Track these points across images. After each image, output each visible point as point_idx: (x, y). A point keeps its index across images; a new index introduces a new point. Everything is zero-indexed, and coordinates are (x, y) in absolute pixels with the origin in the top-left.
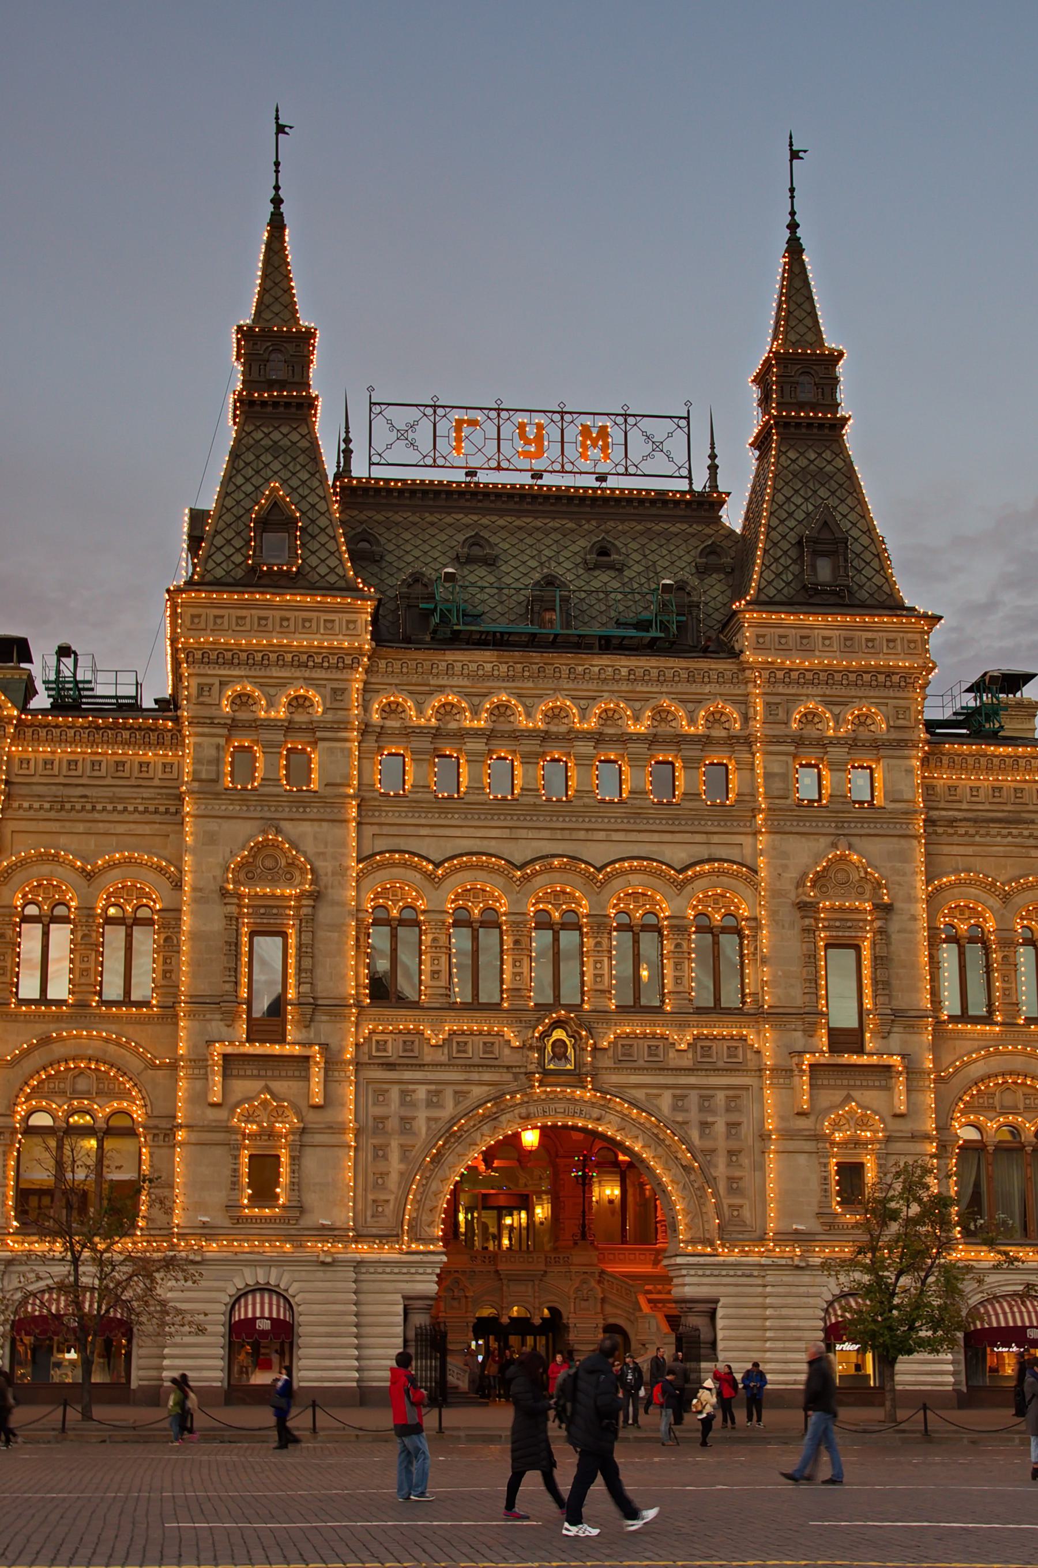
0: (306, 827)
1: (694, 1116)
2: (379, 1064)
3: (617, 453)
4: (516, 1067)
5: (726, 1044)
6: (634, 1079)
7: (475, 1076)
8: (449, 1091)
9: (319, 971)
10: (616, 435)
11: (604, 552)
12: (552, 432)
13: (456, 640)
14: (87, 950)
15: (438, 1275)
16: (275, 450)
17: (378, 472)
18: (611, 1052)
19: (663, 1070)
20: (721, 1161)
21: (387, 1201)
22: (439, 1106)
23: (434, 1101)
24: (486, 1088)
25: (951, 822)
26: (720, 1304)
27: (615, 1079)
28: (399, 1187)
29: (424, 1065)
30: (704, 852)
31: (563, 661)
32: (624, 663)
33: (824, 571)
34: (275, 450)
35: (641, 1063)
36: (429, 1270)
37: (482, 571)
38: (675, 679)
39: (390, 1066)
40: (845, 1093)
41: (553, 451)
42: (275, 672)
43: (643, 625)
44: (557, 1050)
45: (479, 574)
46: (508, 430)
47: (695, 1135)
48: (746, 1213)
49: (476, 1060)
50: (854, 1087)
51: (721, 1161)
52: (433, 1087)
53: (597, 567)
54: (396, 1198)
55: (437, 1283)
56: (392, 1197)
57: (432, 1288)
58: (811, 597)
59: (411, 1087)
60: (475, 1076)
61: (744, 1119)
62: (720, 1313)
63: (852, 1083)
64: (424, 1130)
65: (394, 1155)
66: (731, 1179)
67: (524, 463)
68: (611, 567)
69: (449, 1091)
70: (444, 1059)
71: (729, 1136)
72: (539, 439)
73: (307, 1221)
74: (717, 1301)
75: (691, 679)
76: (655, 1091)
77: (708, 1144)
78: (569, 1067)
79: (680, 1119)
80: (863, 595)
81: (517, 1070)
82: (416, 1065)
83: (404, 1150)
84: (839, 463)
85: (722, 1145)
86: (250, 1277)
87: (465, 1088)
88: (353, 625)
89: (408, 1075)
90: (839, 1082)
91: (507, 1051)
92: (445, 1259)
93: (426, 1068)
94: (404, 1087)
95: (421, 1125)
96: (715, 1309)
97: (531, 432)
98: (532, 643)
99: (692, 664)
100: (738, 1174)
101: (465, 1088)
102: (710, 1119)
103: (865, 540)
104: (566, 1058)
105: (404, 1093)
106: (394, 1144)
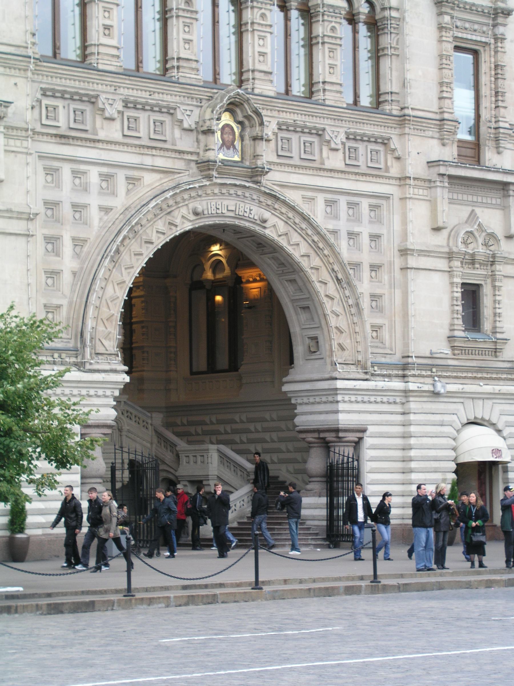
2: (52, 135)
4: (188, 153)
5: (372, 146)
6: (295, 178)
7: (148, 161)
8: (121, 176)
15: (115, 399)
18: (272, 144)
21: (59, 307)
24: (156, 176)
26: (368, 433)
28: (73, 291)
29: (99, 141)
35: (296, 161)
36: (108, 393)
40: (470, 209)
44: (225, 136)
49: (145, 142)
50: (474, 204)
52: (105, 170)
54: (70, 303)
55: (114, 407)
56: (64, 302)
59: (83, 167)
60: (148, 161)
61: (383, 231)
62: (368, 441)
63: (475, 199)
64: (96, 222)
65: (67, 248)
66: (374, 297)
69: (121, 176)
70: (117, 136)
74: (364, 431)
76: (310, 194)
77: (355, 258)
78: (237, 158)
79: (331, 227)
81: (189, 157)
82: (86, 140)
83: (78, 242)
87: (136, 174)
90: (465, 197)
91: (177, 133)
92: (127, 379)
93: (100, 145)
94: (76, 166)
95: (94, 215)
96: (361, 439)
100: (378, 291)
101: (136, 174)
102: (356, 229)
104: (234, 147)
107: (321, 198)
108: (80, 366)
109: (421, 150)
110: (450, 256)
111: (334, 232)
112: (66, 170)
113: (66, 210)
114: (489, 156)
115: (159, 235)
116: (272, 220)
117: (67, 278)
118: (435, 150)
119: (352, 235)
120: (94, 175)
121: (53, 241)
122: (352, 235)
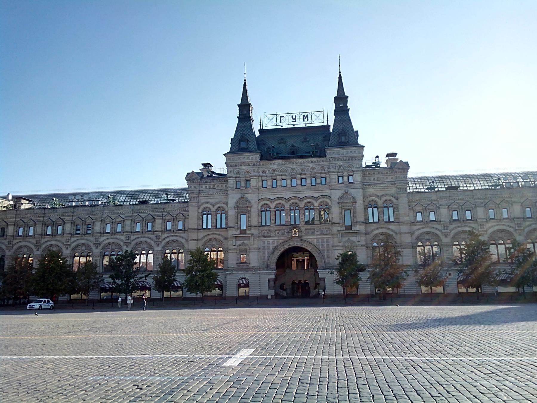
0: (249, 195)
1: (320, 243)
3: (310, 119)
8: (276, 241)
9: (252, 221)
10: (310, 116)
11: (305, 139)
12: (298, 117)
13: (276, 159)
14: (215, 219)
16: (244, 127)
17: (267, 128)
19: (314, 235)
20: (326, 251)
22: (274, 244)
23: (273, 243)
25: (369, 185)
27: (305, 237)
30: (321, 194)
31: (294, 161)
32: (305, 160)
33: (343, 139)
34: (244, 127)
37: (283, 145)
38: (315, 162)
39: (265, 237)
41: (298, 120)
42: (243, 167)
43: (309, 152)
45: (282, 145)
46: (290, 117)
47: (321, 247)
48: (331, 262)
51: (326, 251)
53: (304, 142)
57: (273, 277)
58: (341, 145)
67: (293, 123)
68: (307, 141)
69: (276, 241)
71: (327, 247)
72: (295, 119)
73: (250, 266)
75: (318, 162)
80: (351, 143)
84: (347, 118)
85: (325, 248)
86: (241, 276)
88: (256, 157)
89: (268, 238)
95: (271, 248)
97: (294, 117)
98: (288, 158)
99: (317, 159)
103: (352, 132)
105: (268, 242)
106: (266, 251)
107: (315, 240)
108: (267, 270)
109: (337, 229)
110: (342, 246)
111: (319, 245)
112: (266, 241)
113: (266, 247)
114: (353, 228)
115: (282, 249)
116: (304, 244)
117: (266, 257)
118: (339, 229)
119: (322, 245)
120: (271, 241)
121: (264, 253)
122: (322, 245)
